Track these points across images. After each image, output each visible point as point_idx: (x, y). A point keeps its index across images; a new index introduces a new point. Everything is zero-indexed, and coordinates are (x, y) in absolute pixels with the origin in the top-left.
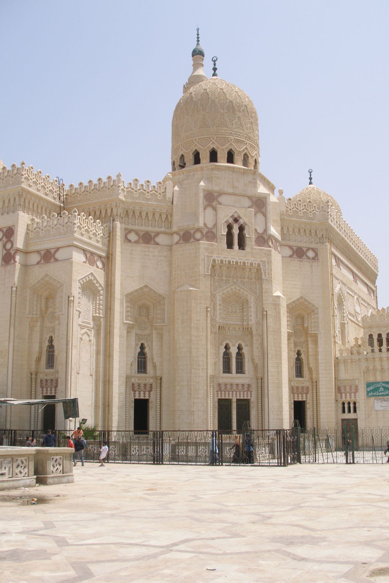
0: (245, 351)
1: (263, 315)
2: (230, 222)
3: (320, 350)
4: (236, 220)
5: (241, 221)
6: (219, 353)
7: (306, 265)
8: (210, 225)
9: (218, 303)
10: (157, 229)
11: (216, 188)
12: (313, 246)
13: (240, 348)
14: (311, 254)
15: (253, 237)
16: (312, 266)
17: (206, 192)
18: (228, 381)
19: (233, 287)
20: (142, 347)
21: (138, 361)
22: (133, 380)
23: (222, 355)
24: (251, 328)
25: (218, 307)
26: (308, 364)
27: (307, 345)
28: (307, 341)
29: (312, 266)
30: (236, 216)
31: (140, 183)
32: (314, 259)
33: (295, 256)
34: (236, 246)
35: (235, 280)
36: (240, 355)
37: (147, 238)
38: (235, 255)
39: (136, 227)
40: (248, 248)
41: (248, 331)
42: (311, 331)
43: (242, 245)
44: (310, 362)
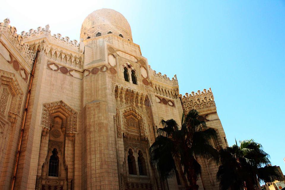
4: (129, 66)
5: (133, 68)
12: (171, 99)
13: (140, 154)
14: (171, 104)
17: (108, 47)
18: (134, 180)
20: (55, 152)
21: (50, 165)
22: (44, 182)
38: (130, 85)
39: (57, 62)
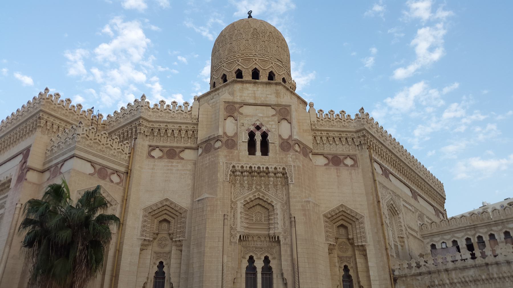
0: (273, 264)
1: (292, 221)
2: (252, 129)
3: (370, 264)
4: (258, 128)
5: (264, 129)
6: (240, 268)
7: (344, 172)
8: (230, 133)
9: (239, 210)
10: (182, 145)
11: (238, 99)
12: (352, 152)
13: (267, 260)
14: (349, 162)
15: (277, 143)
16: (351, 174)
19: (256, 194)
23: (245, 269)
24: (278, 237)
25: (239, 216)
26: (359, 282)
27: (355, 259)
28: (355, 255)
29: (351, 174)
30: (258, 124)
31: (166, 104)
32: (352, 166)
33: (331, 164)
34: (258, 153)
35: (258, 187)
36: (267, 270)
37: (172, 154)
38: (258, 160)
40: (271, 154)
41: (276, 240)
42: (358, 242)
43: (265, 151)
44: (360, 280)
